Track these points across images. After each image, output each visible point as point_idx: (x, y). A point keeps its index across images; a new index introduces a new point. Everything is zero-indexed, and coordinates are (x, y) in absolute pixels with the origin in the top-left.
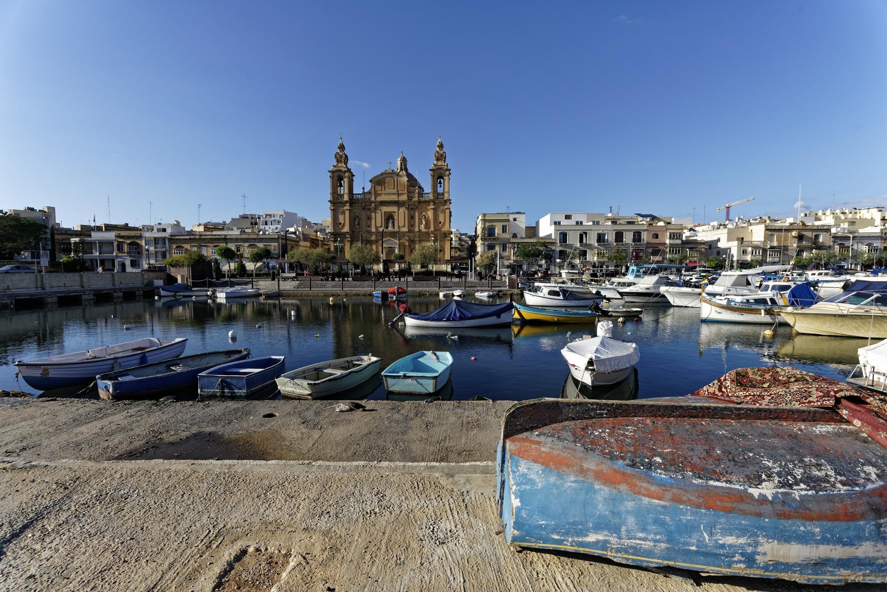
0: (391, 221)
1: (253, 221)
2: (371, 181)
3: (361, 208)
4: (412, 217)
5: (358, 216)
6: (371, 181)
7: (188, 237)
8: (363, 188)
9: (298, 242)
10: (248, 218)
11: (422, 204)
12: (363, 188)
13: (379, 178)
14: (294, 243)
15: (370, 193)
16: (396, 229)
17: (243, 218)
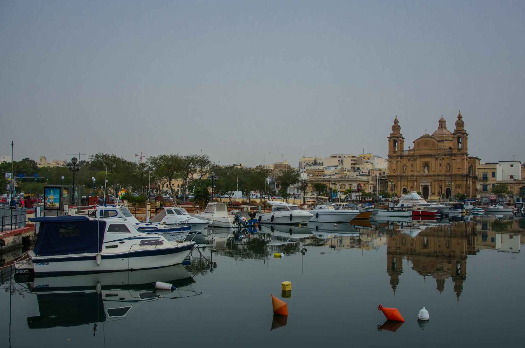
0: (426, 168)
1: (340, 159)
2: (414, 142)
3: (407, 160)
4: (440, 165)
5: (405, 165)
6: (414, 142)
7: (310, 180)
8: (409, 147)
9: (368, 182)
10: (336, 157)
11: (447, 156)
12: (409, 147)
13: (419, 141)
14: (366, 183)
15: (413, 150)
16: (429, 174)
17: (333, 157)
